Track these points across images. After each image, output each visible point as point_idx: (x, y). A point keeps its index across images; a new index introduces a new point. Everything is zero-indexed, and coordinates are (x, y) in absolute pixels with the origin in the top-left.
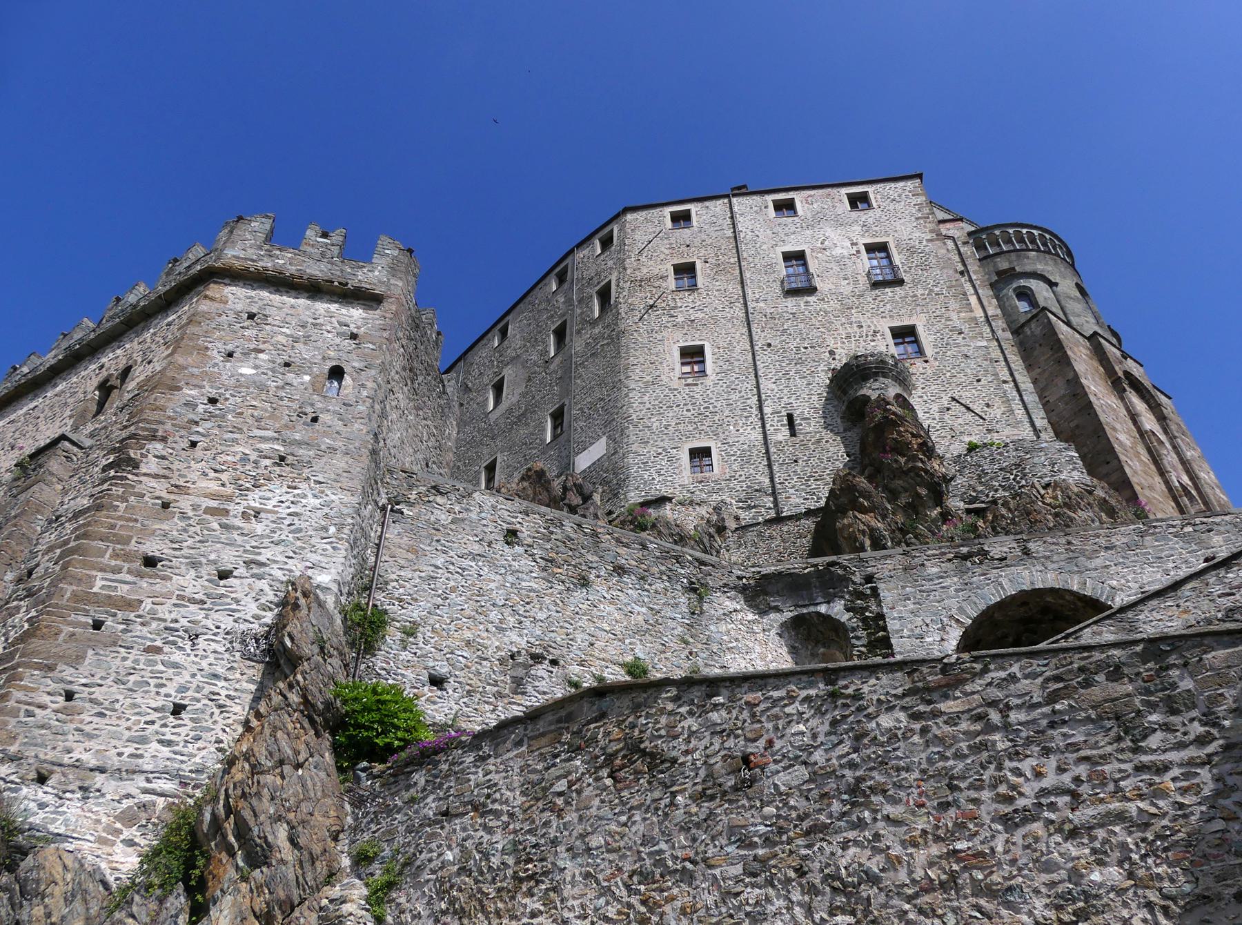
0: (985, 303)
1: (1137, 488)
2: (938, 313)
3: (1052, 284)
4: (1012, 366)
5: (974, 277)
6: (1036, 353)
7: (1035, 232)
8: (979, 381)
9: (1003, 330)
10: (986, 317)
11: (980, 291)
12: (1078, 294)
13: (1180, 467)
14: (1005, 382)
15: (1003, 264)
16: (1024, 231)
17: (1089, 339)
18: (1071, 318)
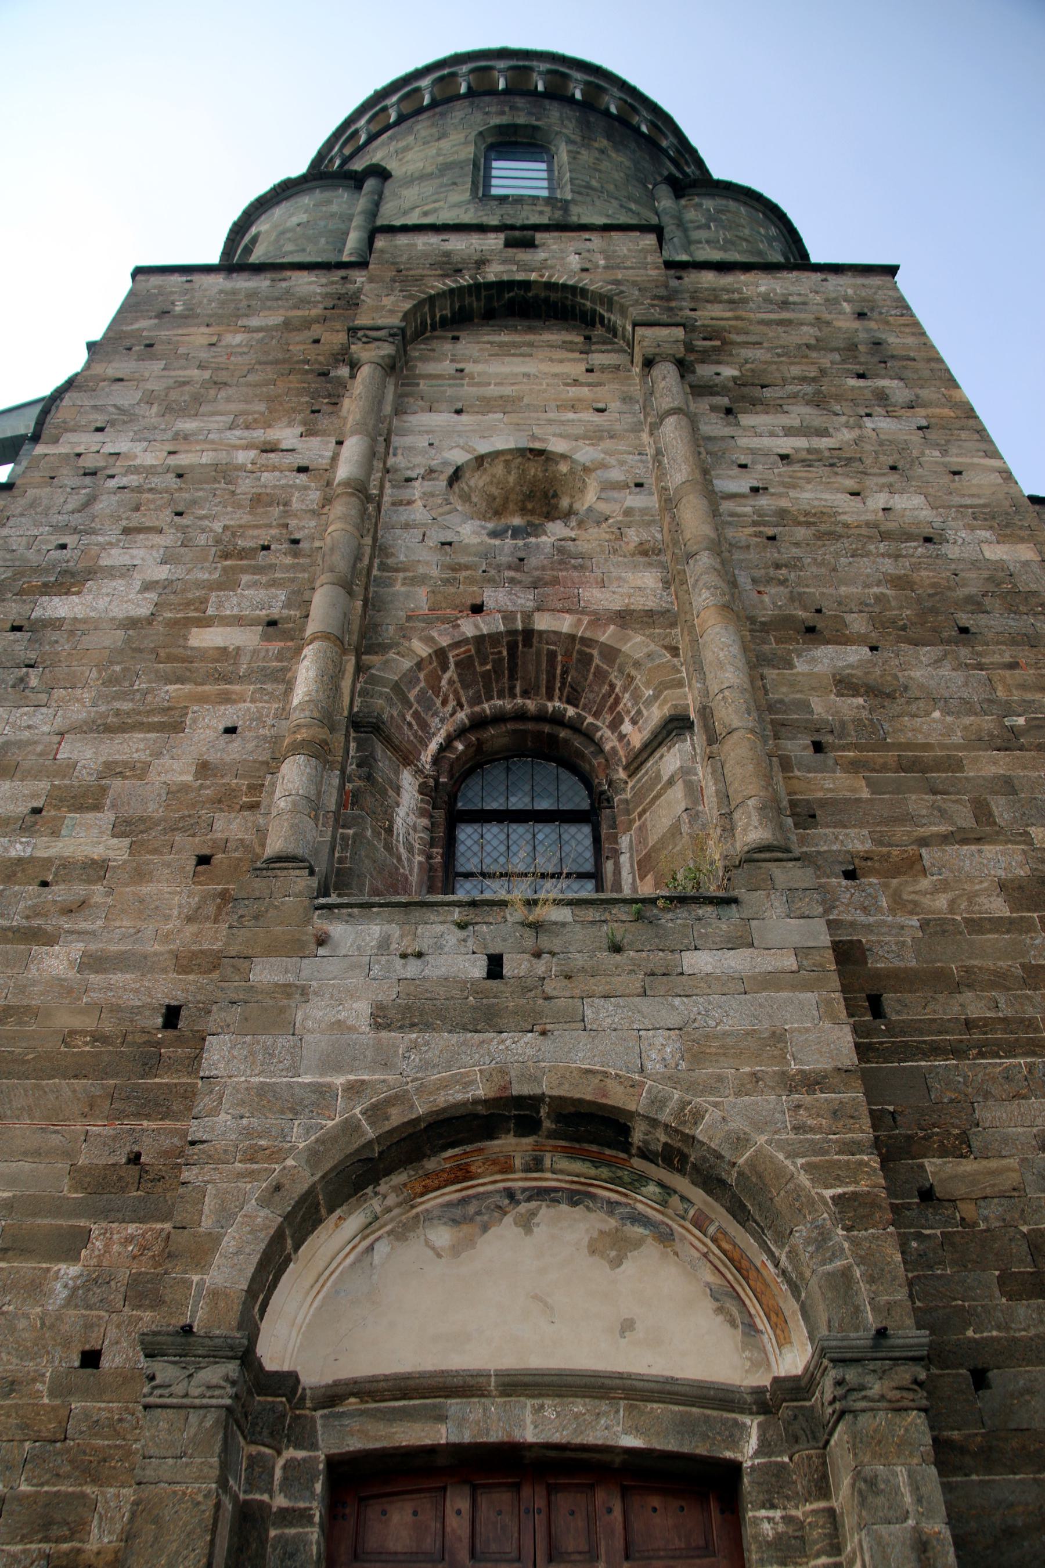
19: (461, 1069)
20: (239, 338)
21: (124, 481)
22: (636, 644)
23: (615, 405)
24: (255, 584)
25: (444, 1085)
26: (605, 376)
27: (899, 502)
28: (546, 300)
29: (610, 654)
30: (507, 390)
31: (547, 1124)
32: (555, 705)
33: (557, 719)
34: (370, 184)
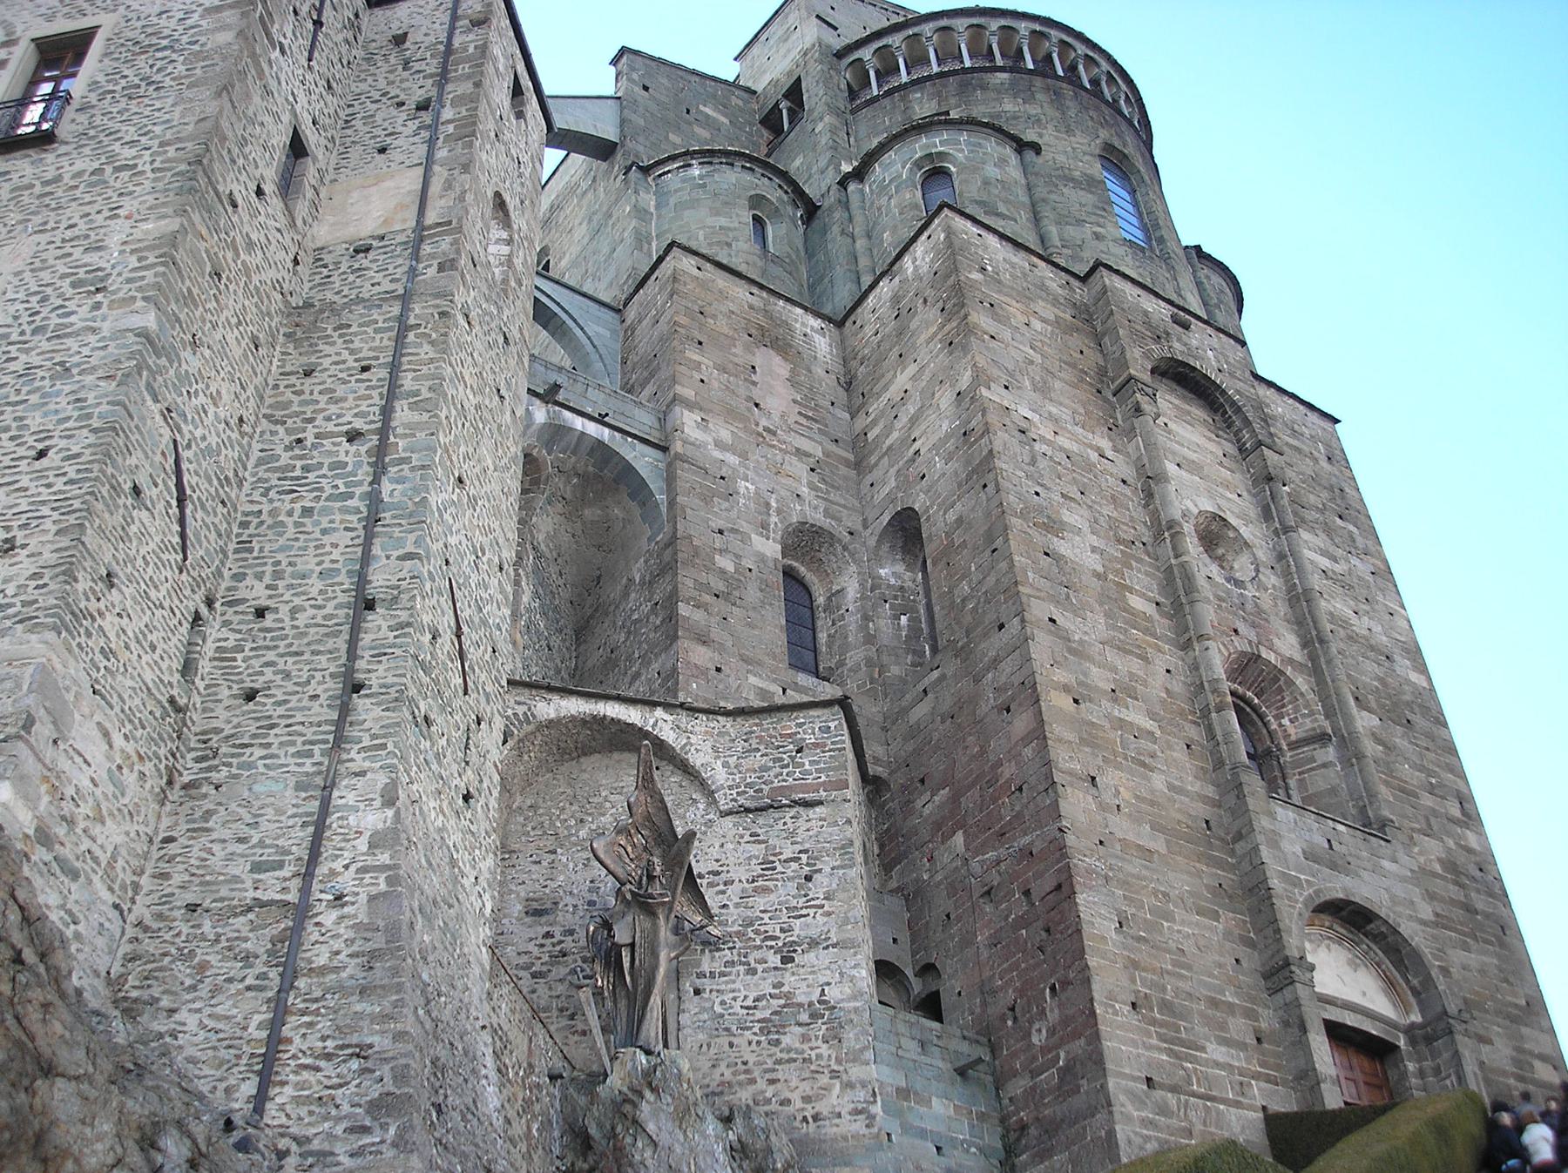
0: (436, 187)
1: (1056, 702)
2: (82, 226)
3: (1021, 146)
4: (407, 382)
5: (447, 113)
6: (913, 326)
7: (1023, 27)
8: (42, 454)
9: (441, 268)
10: (420, 226)
11: (441, 154)
12: (1097, 169)
13: (1283, 608)
14: (353, 436)
15: (923, 106)
16: (995, 24)
17: (1084, 279)
18: (1053, 231)
19: (1337, 886)
20: (1037, 325)
21: (1044, 448)
22: (1302, 682)
23: (1245, 494)
24: (1139, 571)
25: (1330, 889)
26: (1234, 466)
27: (1372, 624)
28: (1197, 383)
29: (1290, 682)
30: (1194, 456)
31: (1344, 913)
32: (1249, 694)
33: (1248, 702)
34: (1029, 155)
